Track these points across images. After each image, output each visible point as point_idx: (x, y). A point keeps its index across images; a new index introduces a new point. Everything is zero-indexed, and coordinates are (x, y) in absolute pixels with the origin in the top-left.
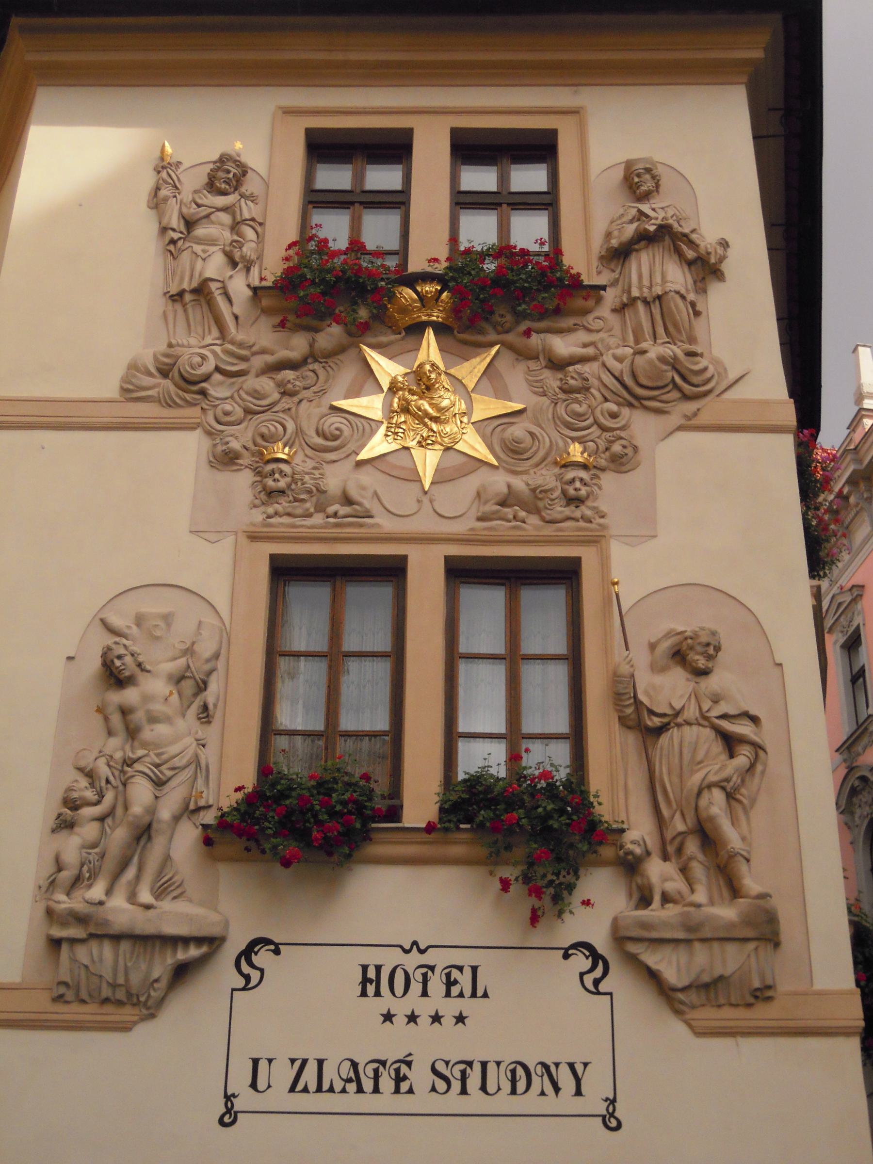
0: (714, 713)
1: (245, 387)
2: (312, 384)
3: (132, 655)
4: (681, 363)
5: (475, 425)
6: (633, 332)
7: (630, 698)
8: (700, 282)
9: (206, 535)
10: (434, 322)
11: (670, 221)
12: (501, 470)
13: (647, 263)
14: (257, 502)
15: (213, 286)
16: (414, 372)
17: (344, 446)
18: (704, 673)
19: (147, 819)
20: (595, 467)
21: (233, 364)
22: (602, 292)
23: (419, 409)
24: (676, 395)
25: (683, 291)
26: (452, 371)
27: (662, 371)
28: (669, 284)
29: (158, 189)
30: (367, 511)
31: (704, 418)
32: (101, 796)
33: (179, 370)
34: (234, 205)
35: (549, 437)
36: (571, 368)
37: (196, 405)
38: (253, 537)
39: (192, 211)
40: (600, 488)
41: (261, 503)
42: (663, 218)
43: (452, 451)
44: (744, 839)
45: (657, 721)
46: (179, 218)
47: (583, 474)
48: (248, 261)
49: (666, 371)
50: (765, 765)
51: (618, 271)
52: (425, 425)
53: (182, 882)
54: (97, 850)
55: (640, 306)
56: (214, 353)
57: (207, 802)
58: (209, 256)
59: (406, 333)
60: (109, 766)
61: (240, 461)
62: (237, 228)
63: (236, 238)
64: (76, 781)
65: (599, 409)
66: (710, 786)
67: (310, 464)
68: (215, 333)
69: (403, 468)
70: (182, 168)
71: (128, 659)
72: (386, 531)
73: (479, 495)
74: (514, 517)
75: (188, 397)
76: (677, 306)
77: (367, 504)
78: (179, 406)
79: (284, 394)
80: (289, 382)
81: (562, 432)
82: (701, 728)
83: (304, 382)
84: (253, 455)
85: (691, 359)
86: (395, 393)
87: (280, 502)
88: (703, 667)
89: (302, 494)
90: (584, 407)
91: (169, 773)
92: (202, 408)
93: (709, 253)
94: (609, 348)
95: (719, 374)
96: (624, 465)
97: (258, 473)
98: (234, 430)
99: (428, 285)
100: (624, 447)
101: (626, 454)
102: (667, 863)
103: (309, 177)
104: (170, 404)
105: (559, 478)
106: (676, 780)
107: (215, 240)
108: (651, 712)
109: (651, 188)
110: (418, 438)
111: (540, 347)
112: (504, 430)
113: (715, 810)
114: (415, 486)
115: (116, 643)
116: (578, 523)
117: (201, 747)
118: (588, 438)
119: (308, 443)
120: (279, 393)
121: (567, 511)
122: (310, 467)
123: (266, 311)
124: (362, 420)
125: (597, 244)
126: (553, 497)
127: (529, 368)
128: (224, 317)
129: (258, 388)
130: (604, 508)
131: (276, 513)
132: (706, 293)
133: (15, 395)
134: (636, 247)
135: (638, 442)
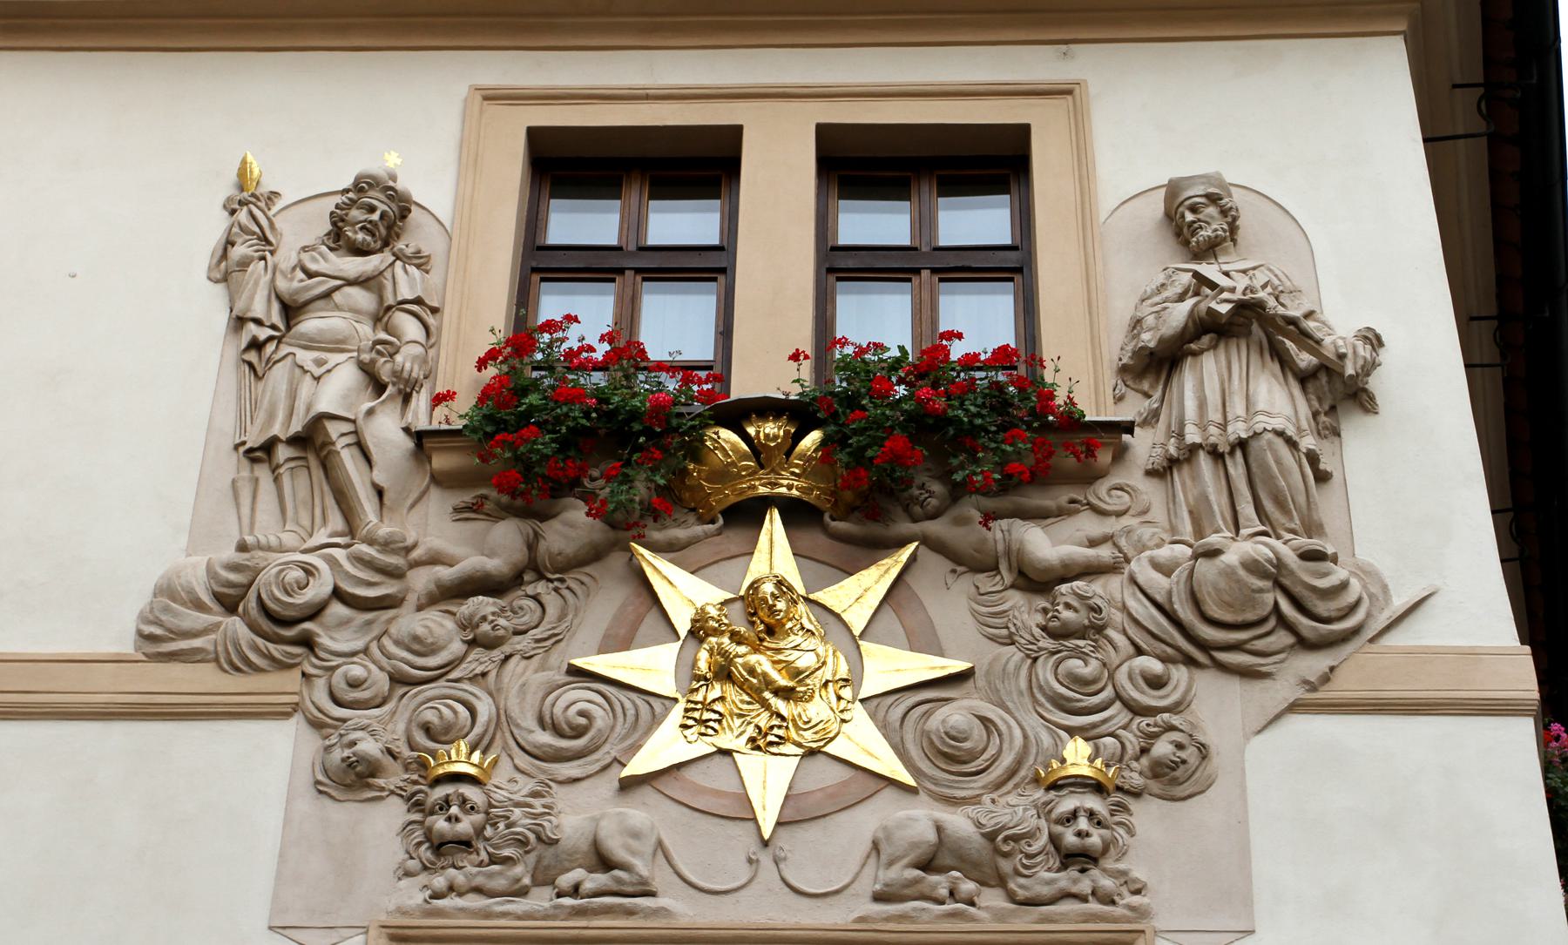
1: (393, 630)
2: (533, 624)
4: (1292, 573)
6: (1191, 512)
8: (1326, 414)
10: (781, 497)
11: (1261, 295)
12: (923, 796)
13: (1216, 378)
14: (413, 865)
15: (334, 429)
16: (742, 598)
17: (597, 749)
20: (1119, 789)
21: (370, 584)
22: (1126, 437)
23: (752, 671)
24: (1283, 638)
26: (824, 596)
27: (1254, 591)
28: (1260, 418)
29: (230, 243)
30: (644, 882)
31: (1346, 686)
33: (259, 597)
34: (381, 273)
35: (1022, 729)
36: (1064, 588)
37: (291, 667)
39: (295, 284)
40: (1131, 832)
41: (420, 866)
42: (1246, 289)
43: (820, 761)
46: (269, 301)
47: (1092, 802)
48: (407, 381)
49: (1261, 591)
51: (1157, 395)
52: (765, 705)
55: (1204, 462)
56: (333, 562)
58: (329, 371)
61: (380, 782)
62: (386, 319)
63: (383, 336)
67: (526, 785)
68: (336, 521)
69: (718, 793)
70: (279, 204)
72: (683, 922)
73: (876, 846)
74: (952, 893)
76: (1278, 462)
77: (642, 867)
78: (258, 670)
79: (472, 643)
80: (484, 618)
83: (515, 621)
84: (407, 768)
86: (701, 641)
87: (461, 864)
89: (509, 846)
92: (304, 674)
93: (1342, 357)
94: (1144, 548)
95: (1371, 596)
97: (417, 805)
99: (771, 425)
100: (1180, 746)
101: (1184, 762)
103: (533, 222)
104: (239, 665)
105: (1044, 810)
110: (750, 731)
111: (1000, 547)
112: (927, 715)
114: (742, 831)
119: (520, 740)
121: (1065, 879)
122: (525, 792)
123: (440, 480)
124: (634, 696)
125: (1115, 347)
127: (977, 588)
128: (354, 488)
129: (420, 631)
130: (1139, 873)
131: (451, 888)
132: (1339, 435)
134: (1193, 346)
135: (1209, 736)
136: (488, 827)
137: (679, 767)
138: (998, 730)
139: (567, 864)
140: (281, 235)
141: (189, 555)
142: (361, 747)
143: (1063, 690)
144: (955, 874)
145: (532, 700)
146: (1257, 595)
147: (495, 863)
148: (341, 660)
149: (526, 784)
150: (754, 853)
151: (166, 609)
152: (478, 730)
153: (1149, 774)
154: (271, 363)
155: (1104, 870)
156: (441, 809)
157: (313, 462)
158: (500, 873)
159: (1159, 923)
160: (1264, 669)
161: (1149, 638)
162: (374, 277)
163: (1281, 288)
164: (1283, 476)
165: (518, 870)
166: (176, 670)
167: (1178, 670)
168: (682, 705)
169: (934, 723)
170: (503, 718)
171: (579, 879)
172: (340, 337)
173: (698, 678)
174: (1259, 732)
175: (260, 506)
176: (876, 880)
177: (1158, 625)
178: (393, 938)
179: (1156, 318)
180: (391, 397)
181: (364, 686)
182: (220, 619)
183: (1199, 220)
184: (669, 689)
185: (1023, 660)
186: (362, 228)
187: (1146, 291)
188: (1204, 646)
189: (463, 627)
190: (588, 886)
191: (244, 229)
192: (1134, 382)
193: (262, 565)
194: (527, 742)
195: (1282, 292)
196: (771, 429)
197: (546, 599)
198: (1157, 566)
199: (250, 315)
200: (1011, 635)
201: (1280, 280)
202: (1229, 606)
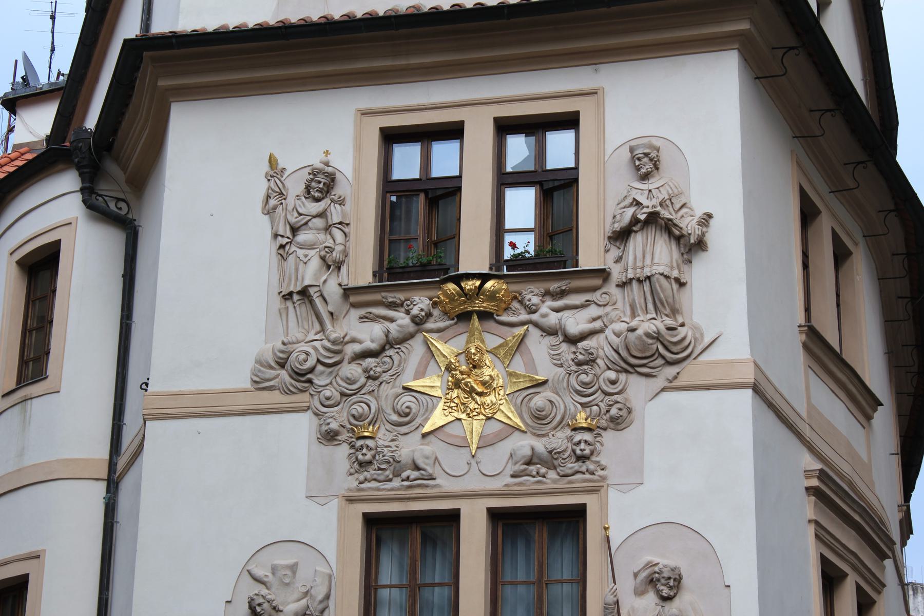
1: (340, 374)
2: (389, 368)
3: (269, 602)
4: (663, 336)
5: (509, 396)
6: (630, 305)
8: (687, 253)
11: (659, 209)
14: (352, 471)
15: (312, 291)
20: (598, 427)
23: (466, 384)
24: (660, 361)
27: (648, 345)
28: (654, 267)
29: (268, 197)
30: (431, 475)
31: (682, 381)
34: (326, 210)
37: (305, 391)
38: (351, 500)
40: (602, 445)
42: (653, 206)
43: (493, 420)
47: (587, 436)
48: (338, 263)
49: (652, 344)
51: (622, 248)
52: (474, 399)
55: (634, 282)
56: (315, 348)
58: (309, 260)
59: (457, 319)
61: (339, 438)
65: (602, 377)
67: (391, 436)
68: (317, 327)
71: (266, 605)
72: (443, 490)
73: (511, 455)
74: (538, 473)
75: (299, 385)
76: (661, 286)
77: (430, 470)
78: (294, 393)
79: (369, 378)
80: (371, 369)
81: (574, 398)
83: (383, 367)
87: (369, 470)
88: (666, 595)
90: (591, 376)
92: (310, 394)
93: (690, 234)
94: (612, 322)
95: (696, 339)
97: (353, 447)
99: (470, 283)
100: (620, 409)
101: (621, 416)
104: (288, 392)
105: (570, 439)
109: (649, 170)
111: (558, 327)
112: (530, 399)
115: (256, 595)
116: (585, 476)
118: (593, 403)
120: (366, 377)
121: (576, 466)
122: (389, 440)
124: (426, 397)
126: (564, 457)
128: (322, 315)
129: (349, 376)
130: (603, 463)
134: (634, 228)
136: (377, 456)
137: (443, 426)
138: (556, 407)
139: (404, 469)
140: (288, 189)
141: (266, 343)
143: (579, 388)
144: (539, 466)
145: (390, 402)
146: (651, 346)
147: (380, 470)
148: (322, 388)
149: (389, 436)
150: (469, 461)
151: (260, 371)
152: (371, 416)
155: (592, 461)
156: (360, 449)
160: (653, 374)
162: (323, 212)
163: (672, 195)
165: (387, 473)
166: (265, 393)
167: (622, 375)
168: (443, 400)
169: (532, 404)
170: (381, 409)
171: (408, 475)
172: (312, 243)
174: (650, 400)
176: (511, 470)
177: (615, 359)
178: (347, 500)
179: (620, 216)
181: (331, 399)
182: (278, 372)
183: (641, 164)
184: (438, 393)
185: (565, 375)
186: (317, 191)
187: (619, 200)
189: (365, 372)
190: (412, 477)
191: (272, 190)
192: (614, 241)
193: (292, 350)
194: (389, 419)
195: (673, 197)
197: (394, 357)
198: (615, 334)
199: (279, 233)
200: (562, 364)
201: (672, 190)
202: (641, 351)
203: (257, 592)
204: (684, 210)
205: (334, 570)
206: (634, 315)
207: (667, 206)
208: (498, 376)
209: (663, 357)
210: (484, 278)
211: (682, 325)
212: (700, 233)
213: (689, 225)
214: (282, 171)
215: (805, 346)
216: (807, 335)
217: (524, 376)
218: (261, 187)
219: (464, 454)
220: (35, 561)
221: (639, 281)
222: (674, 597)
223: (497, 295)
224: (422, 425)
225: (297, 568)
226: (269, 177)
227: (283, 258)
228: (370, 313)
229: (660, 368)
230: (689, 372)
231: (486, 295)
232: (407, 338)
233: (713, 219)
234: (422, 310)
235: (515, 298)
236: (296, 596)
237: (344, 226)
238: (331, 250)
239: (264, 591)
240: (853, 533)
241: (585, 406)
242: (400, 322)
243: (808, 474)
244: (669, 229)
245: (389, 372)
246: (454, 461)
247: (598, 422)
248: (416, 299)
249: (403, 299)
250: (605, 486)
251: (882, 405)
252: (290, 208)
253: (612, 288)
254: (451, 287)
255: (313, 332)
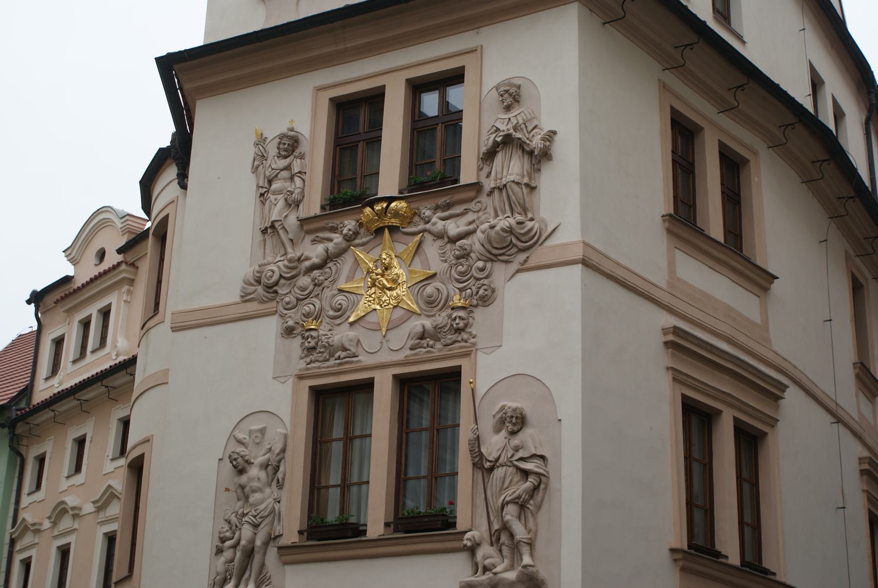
0: (516, 457)
3: (242, 457)
7: (476, 452)
9: (279, 379)
11: (512, 131)
12: (423, 316)
14: (303, 355)
15: (277, 225)
17: (345, 314)
18: (513, 433)
19: (250, 546)
20: (471, 305)
24: (514, 250)
25: (517, 179)
27: (504, 237)
28: (508, 177)
30: (354, 353)
31: (532, 263)
32: (234, 534)
34: (291, 164)
37: (274, 300)
38: (300, 378)
40: (474, 319)
43: (398, 309)
44: (529, 531)
45: (487, 465)
47: (462, 313)
49: (506, 237)
50: (547, 485)
51: (491, 166)
52: (385, 293)
53: (270, 576)
54: (233, 563)
55: (496, 192)
56: (279, 267)
57: (279, 533)
60: (236, 517)
61: (295, 332)
64: (222, 528)
66: (508, 503)
67: (329, 327)
69: (373, 323)
70: (268, 141)
72: (362, 364)
74: (428, 345)
75: (269, 295)
76: (513, 191)
77: (353, 350)
81: (455, 286)
82: (508, 468)
85: (519, 226)
88: (511, 430)
90: (465, 266)
91: (260, 520)
92: (277, 302)
93: (535, 148)
94: (483, 223)
96: (486, 302)
97: (303, 338)
98: (291, 313)
100: (486, 290)
101: (486, 295)
102: (492, 547)
104: (263, 302)
106: (495, 500)
107: (281, 191)
108: (487, 460)
109: (510, 103)
111: (443, 231)
112: (424, 289)
113: (508, 517)
114: (378, 333)
115: (233, 452)
117: (277, 503)
118: (466, 288)
121: (454, 337)
124: (354, 295)
129: (301, 285)
130: (474, 332)
131: (311, 362)
132: (540, 170)
133: (193, 308)
134: (498, 149)
137: (364, 316)
138: (441, 293)
141: (250, 267)
142: (289, 323)
143: (457, 277)
144: (428, 339)
153: (479, 299)
154: (266, 200)
155: (466, 332)
157: (276, 233)
158: (321, 356)
159: (478, 347)
161: (480, 255)
164: (515, 196)
165: (325, 354)
169: (424, 293)
173: (368, 287)
175: (267, 248)
177: (482, 251)
178: (298, 378)
180: (293, 208)
182: (257, 287)
185: (449, 267)
186: (284, 150)
188: (495, 255)
190: (342, 356)
196: (378, 208)
197: (332, 268)
200: (446, 260)
203: (233, 450)
204: (535, 131)
205: (289, 431)
206: (497, 215)
207: (522, 129)
208: (402, 274)
209: (517, 247)
210: (390, 200)
211: (532, 220)
212: (542, 147)
213: (536, 142)
214: (264, 140)
215: (669, 231)
216: (669, 221)
217: (420, 272)
218: (250, 152)
219: (378, 336)
220: (147, 444)
221: (500, 189)
222: (518, 431)
223: (400, 212)
224: (349, 317)
225: (265, 431)
226: (256, 144)
227: (263, 203)
228: (318, 237)
229: (515, 255)
230: (537, 256)
231: (392, 213)
232: (341, 253)
233: (557, 135)
234: (350, 230)
235: (415, 214)
236: (263, 452)
237: (302, 175)
238: (292, 193)
239: (240, 449)
240: (728, 378)
241: (462, 290)
242: (335, 241)
243: (665, 331)
244: (521, 145)
245: (329, 279)
246: (371, 341)
247: (471, 301)
248: (346, 222)
249: (338, 223)
250: (474, 351)
251: (777, 278)
252: (267, 166)
253: (483, 198)
254: (368, 210)
255: (279, 255)
